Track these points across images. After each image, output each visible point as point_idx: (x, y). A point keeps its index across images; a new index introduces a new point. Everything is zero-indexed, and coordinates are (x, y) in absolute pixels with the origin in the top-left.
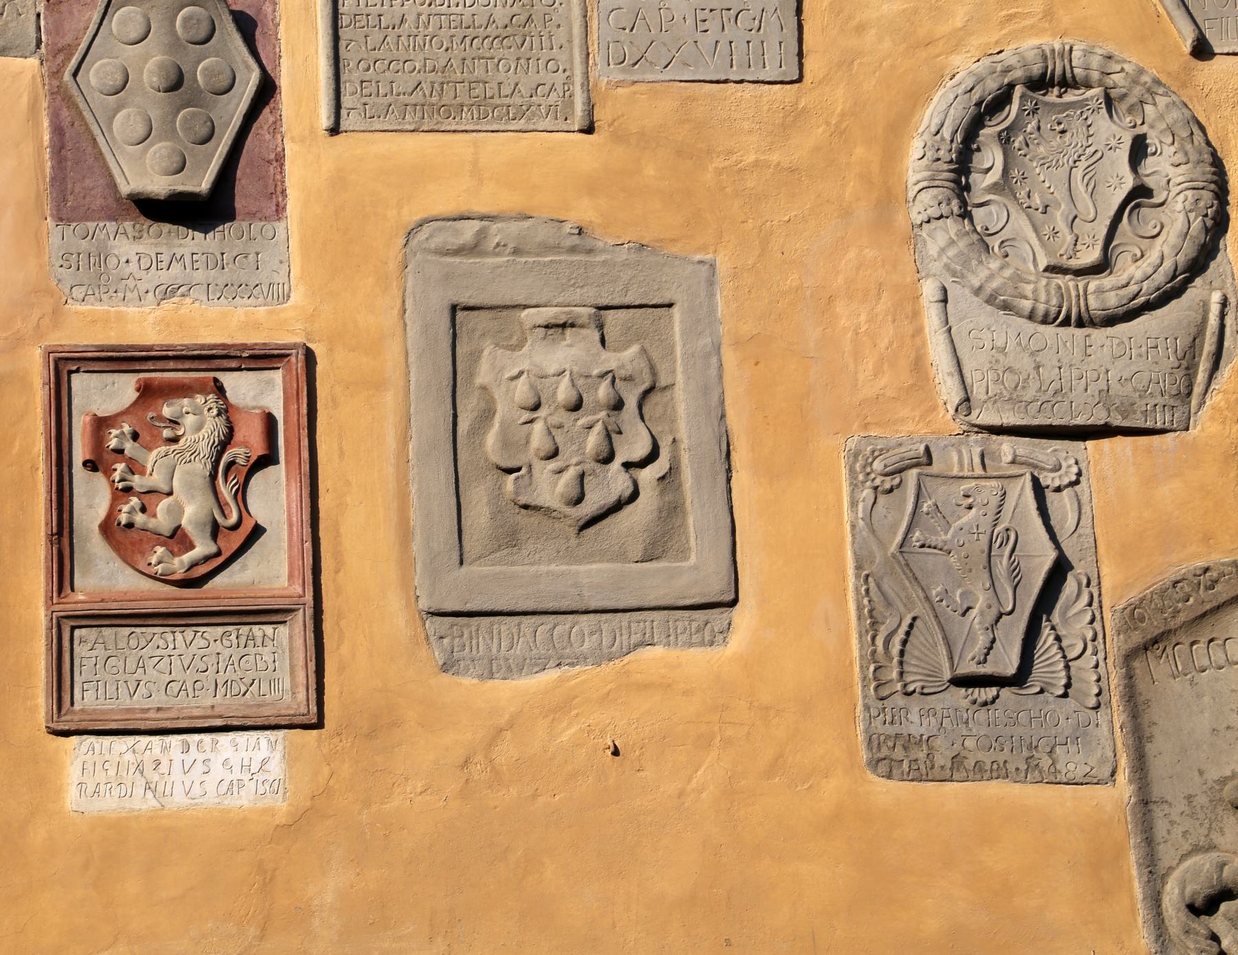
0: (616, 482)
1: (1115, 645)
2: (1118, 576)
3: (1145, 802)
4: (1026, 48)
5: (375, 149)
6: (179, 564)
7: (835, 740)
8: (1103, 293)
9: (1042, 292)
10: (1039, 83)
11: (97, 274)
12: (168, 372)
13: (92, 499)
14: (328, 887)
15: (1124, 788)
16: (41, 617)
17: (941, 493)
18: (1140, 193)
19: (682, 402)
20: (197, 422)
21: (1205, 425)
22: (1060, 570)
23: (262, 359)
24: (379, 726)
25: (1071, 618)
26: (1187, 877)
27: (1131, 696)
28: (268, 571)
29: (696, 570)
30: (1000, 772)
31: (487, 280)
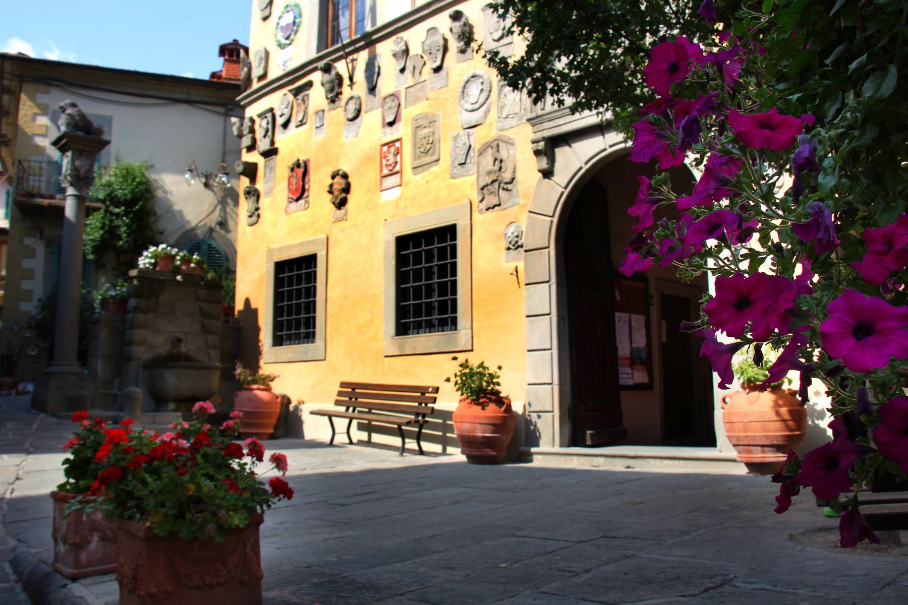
0: (429, 146)
1: (476, 155)
2: (476, 146)
3: (478, 176)
4: (471, 73)
5: (409, 109)
6: (390, 168)
7: (448, 176)
8: (477, 106)
9: (470, 107)
10: (473, 77)
11: (385, 134)
12: (389, 144)
13: (384, 162)
14: (402, 205)
15: (475, 176)
16: (378, 177)
17: (459, 140)
18: (482, 90)
19: (436, 134)
20: (392, 149)
21: (488, 122)
22: (470, 147)
23: (398, 140)
24: (407, 184)
25: (471, 153)
26: (482, 184)
27: (478, 163)
28: (398, 168)
29: (435, 158)
30: (463, 176)
31: (420, 123)
